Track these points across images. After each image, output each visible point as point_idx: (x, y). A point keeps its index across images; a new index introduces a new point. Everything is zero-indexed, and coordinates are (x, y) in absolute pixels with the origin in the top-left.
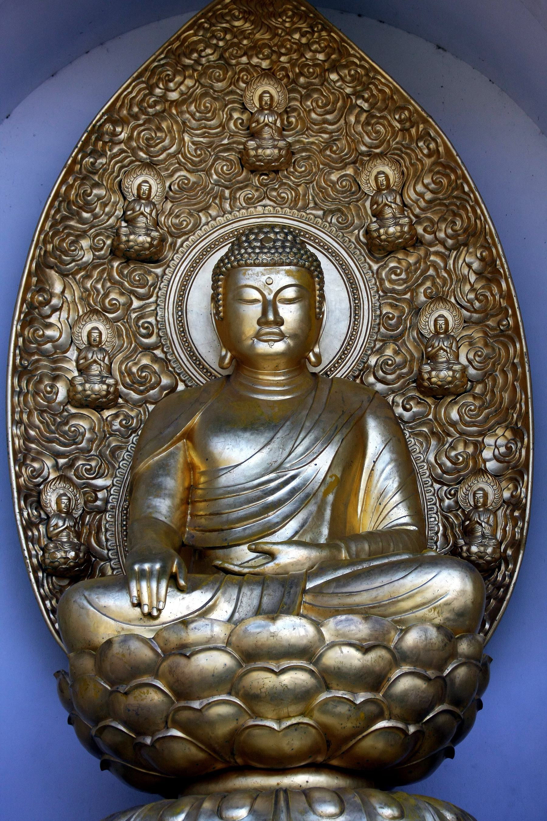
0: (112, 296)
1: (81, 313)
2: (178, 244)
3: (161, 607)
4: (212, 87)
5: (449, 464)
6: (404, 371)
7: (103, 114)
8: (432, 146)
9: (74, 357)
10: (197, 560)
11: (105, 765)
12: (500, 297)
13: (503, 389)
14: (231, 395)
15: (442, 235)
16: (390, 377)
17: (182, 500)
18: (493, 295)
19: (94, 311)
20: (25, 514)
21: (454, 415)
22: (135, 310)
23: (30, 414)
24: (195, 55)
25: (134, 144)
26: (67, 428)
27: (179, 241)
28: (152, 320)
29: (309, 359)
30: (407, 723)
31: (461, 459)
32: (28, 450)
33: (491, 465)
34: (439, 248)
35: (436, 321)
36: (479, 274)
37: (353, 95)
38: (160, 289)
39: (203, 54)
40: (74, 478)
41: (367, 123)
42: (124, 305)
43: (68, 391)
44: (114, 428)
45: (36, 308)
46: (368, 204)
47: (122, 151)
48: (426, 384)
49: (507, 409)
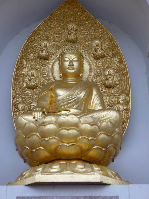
0: (37, 66)
1: (30, 69)
4: (61, 25)
5: (111, 102)
8: (108, 36)
9: (28, 78)
11: (25, 161)
13: (124, 86)
15: (110, 55)
18: (121, 66)
19: (33, 68)
20: (14, 109)
23: (17, 89)
28: (46, 71)
30: (103, 148)
32: (16, 96)
41: (94, 32)
46: (94, 49)
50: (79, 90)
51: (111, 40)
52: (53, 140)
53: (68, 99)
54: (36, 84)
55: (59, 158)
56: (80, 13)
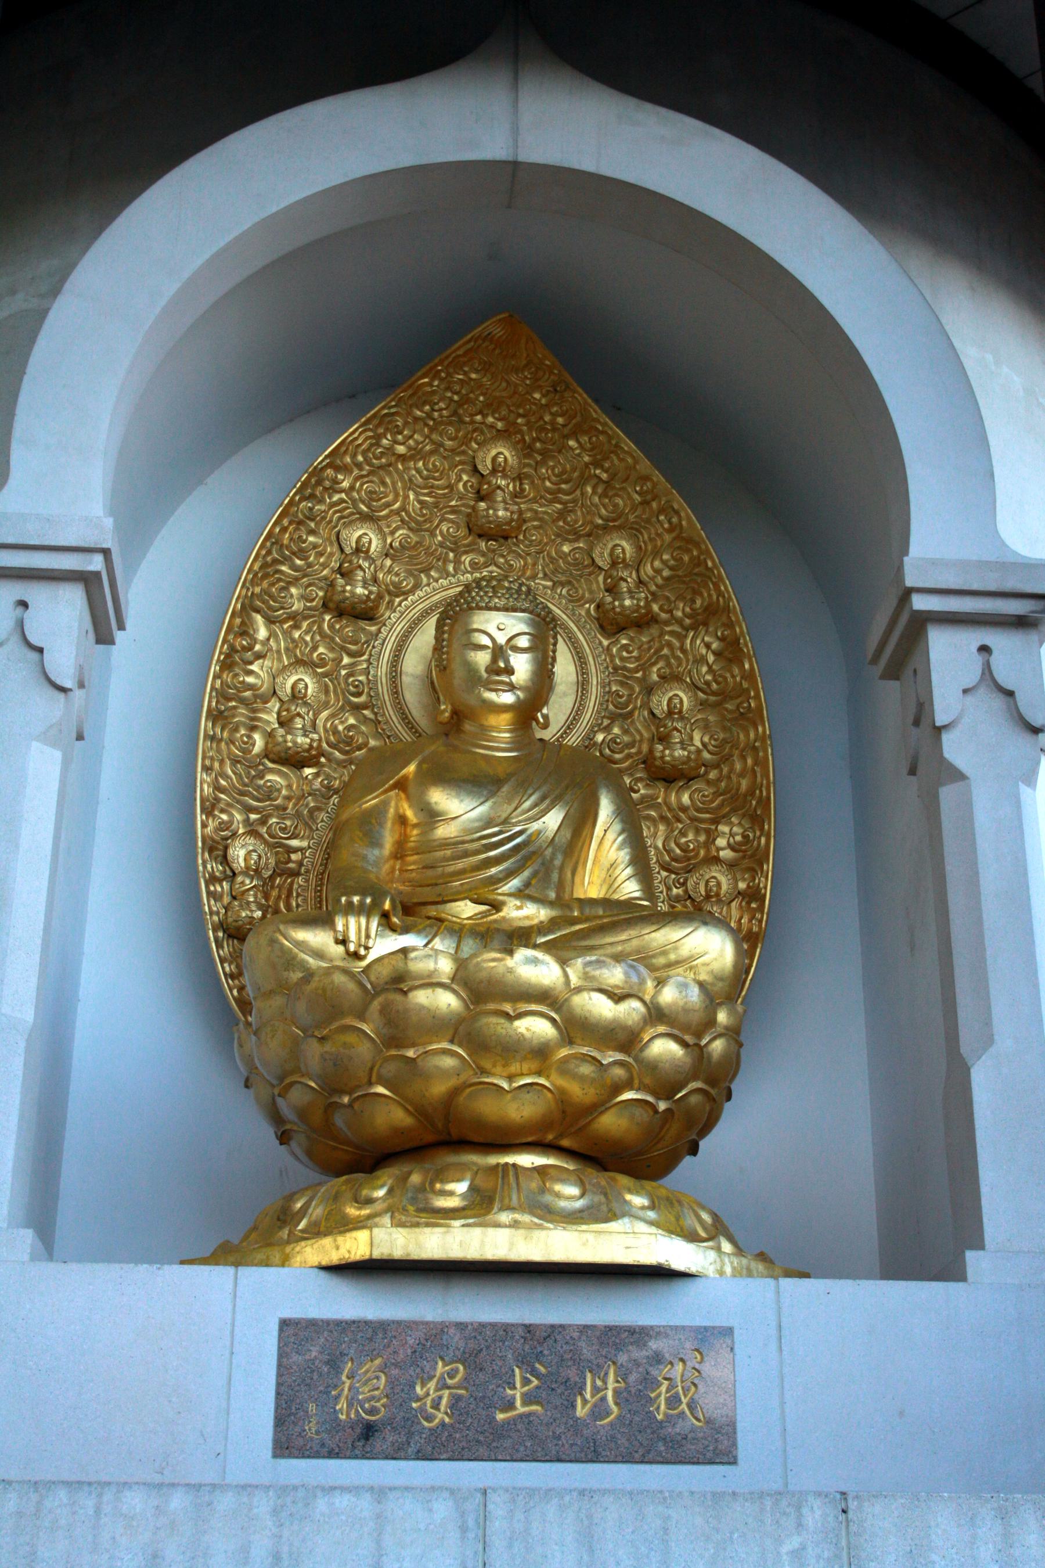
0: (321, 650)
2: (396, 604)
3: (370, 945)
4: (442, 445)
5: (678, 851)
6: (633, 750)
7: (326, 457)
8: (675, 520)
9: (276, 709)
11: (284, 1138)
12: (742, 678)
13: (742, 775)
15: (679, 614)
16: (617, 756)
17: (391, 853)
18: (733, 676)
19: (299, 662)
21: (686, 799)
22: (344, 667)
23: (222, 762)
24: (427, 408)
25: (355, 494)
26: (262, 782)
27: (398, 600)
28: (362, 678)
29: (538, 722)
30: (658, 1098)
31: (692, 846)
32: (218, 800)
33: (726, 854)
34: (677, 628)
35: (670, 700)
36: (717, 654)
37: (592, 464)
38: (374, 647)
39: (436, 407)
40: (266, 836)
41: (604, 495)
42: (333, 661)
43: (267, 744)
44: (314, 787)
45: (237, 651)
46: (601, 578)
47: (342, 501)
48: (658, 763)
49: (745, 796)
50: (533, 798)
51: (684, 541)
52: (448, 1062)
53: (484, 842)
54: (315, 745)
55: (455, 1134)
56: (543, 396)
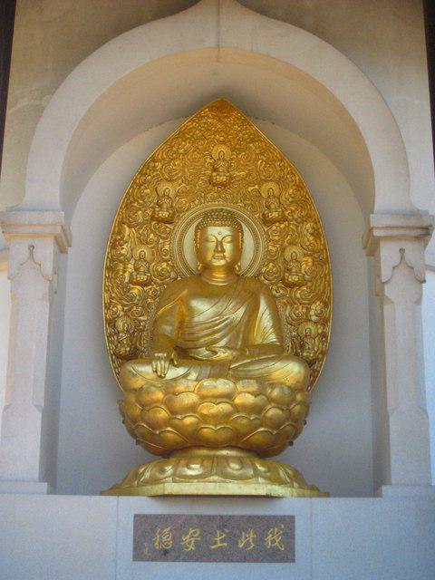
10: (183, 353)
11: (138, 442)
14: (199, 281)
19: (141, 242)
21: (298, 296)
33: (314, 318)
